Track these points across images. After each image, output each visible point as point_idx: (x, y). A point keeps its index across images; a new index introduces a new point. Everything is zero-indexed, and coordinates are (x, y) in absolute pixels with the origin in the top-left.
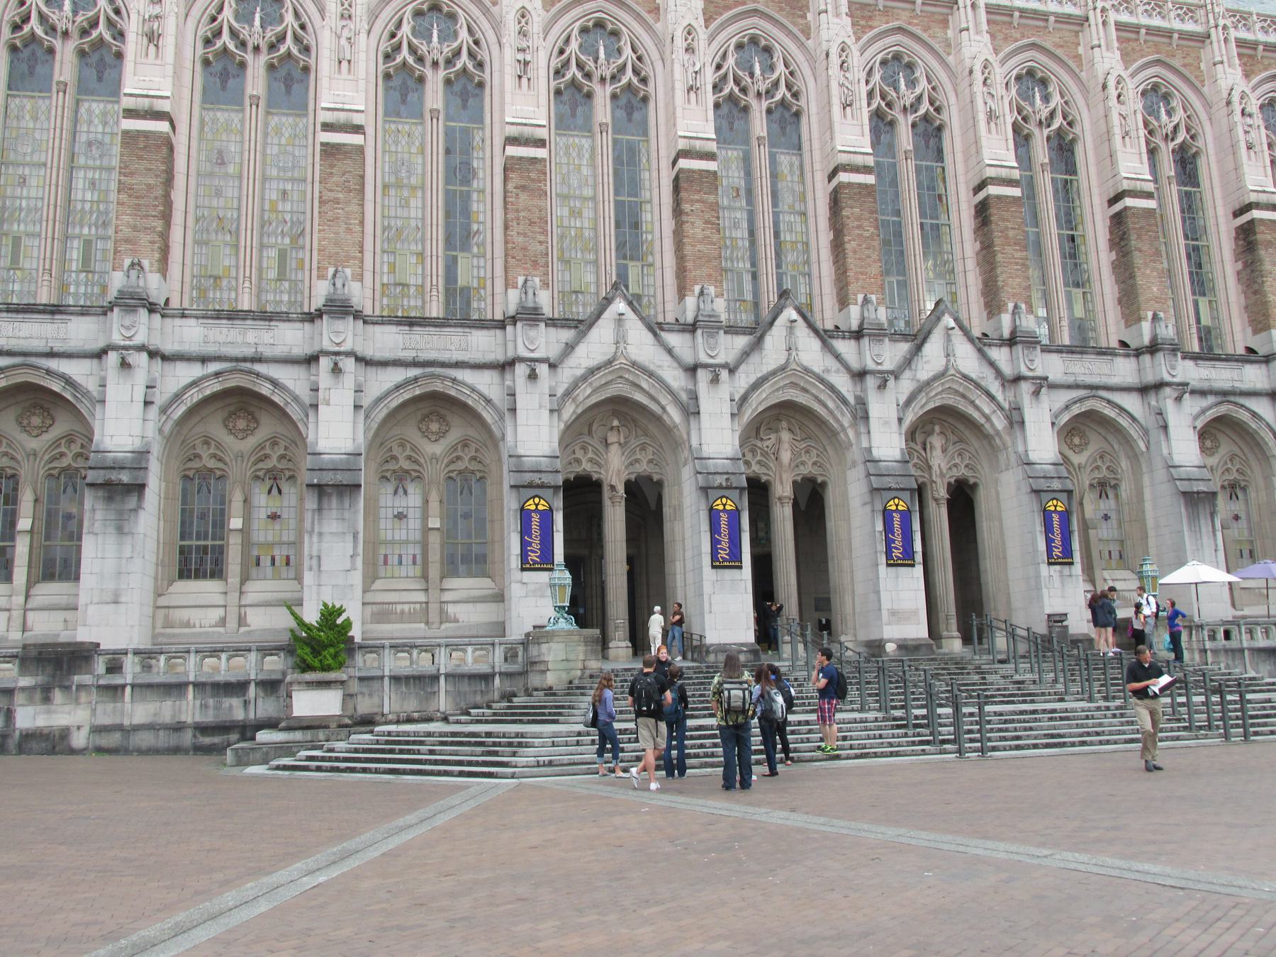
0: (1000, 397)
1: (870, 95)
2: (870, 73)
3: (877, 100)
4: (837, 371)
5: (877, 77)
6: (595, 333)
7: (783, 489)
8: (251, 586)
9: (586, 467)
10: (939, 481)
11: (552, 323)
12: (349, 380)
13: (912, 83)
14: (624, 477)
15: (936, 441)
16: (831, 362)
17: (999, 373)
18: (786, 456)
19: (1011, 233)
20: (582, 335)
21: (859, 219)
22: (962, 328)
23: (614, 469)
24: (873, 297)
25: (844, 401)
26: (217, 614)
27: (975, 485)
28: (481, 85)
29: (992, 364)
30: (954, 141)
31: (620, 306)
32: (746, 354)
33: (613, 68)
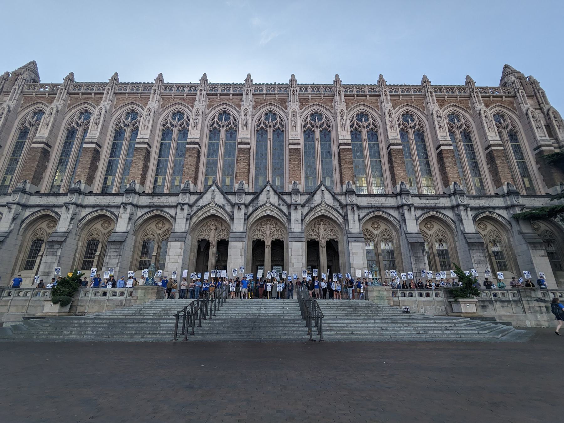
0: (341, 211)
1: (399, 125)
2: (399, 119)
3: (402, 126)
4: (283, 205)
5: (401, 119)
6: (205, 196)
7: (268, 243)
9: (205, 236)
10: (322, 240)
12: (128, 211)
13: (412, 120)
14: (216, 239)
15: (322, 227)
16: (281, 202)
17: (340, 204)
19: (347, 160)
20: (201, 197)
21: (294, 159)
22: (327, 189)
23: (213, 237)
24: (298, 182)
25: (285, 214)
27: (337, 242)
28: (283, 131)
29: (338, 201)
30: (381, 135)
32: (252, 201)
33: (320, 123)
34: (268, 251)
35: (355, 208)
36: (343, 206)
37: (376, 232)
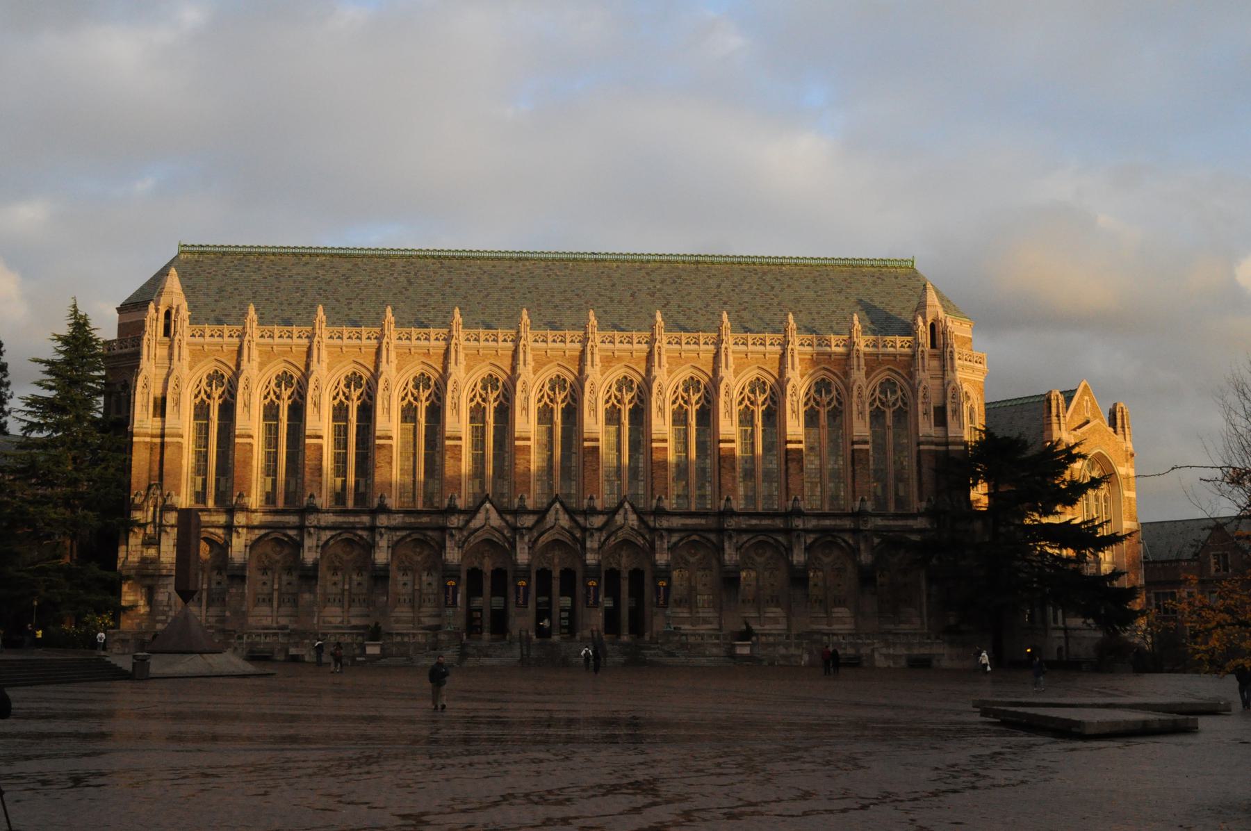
7: (556, 573)
8: (352, 609)
9: (476, 564)
11: (461, 512)
15: (624, 553)
18: (556, 561)
23: (488, 566)
26: (339, 619)
31: (488, 505)
34: (556, 586)
35: (664, 534)
36: (653, 530)
37: (692, 560)
